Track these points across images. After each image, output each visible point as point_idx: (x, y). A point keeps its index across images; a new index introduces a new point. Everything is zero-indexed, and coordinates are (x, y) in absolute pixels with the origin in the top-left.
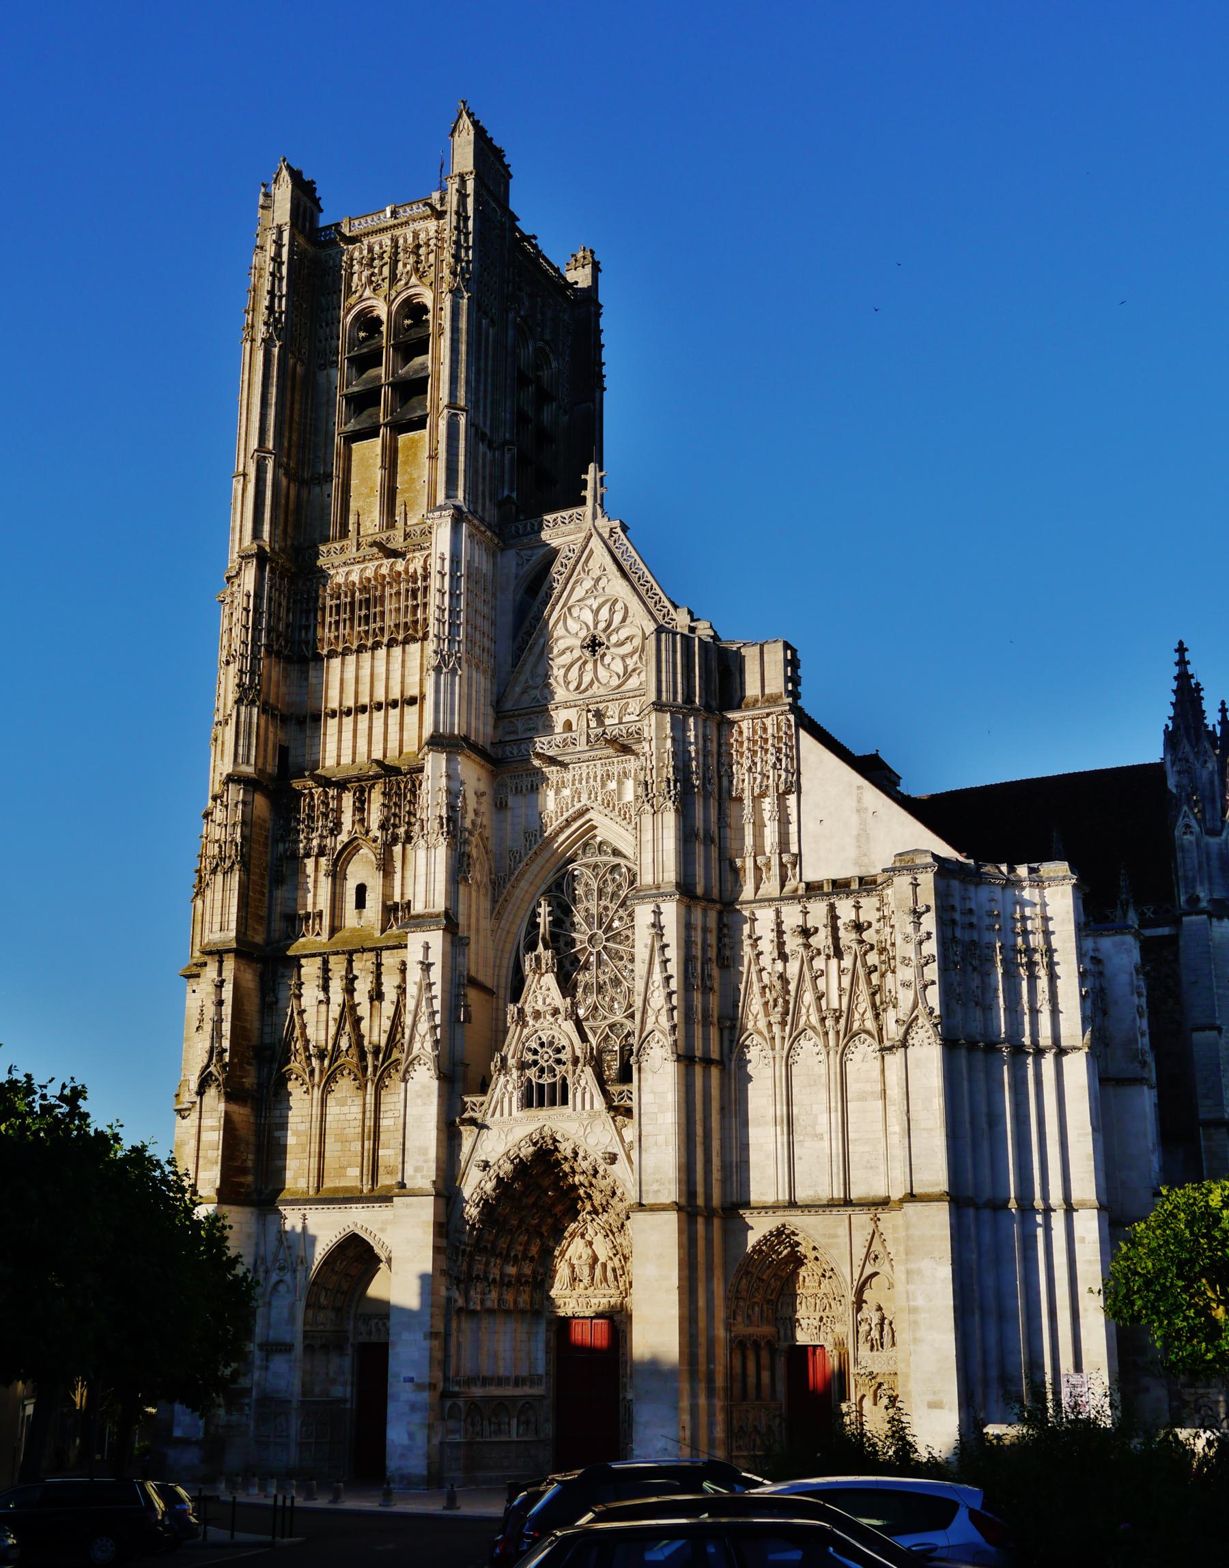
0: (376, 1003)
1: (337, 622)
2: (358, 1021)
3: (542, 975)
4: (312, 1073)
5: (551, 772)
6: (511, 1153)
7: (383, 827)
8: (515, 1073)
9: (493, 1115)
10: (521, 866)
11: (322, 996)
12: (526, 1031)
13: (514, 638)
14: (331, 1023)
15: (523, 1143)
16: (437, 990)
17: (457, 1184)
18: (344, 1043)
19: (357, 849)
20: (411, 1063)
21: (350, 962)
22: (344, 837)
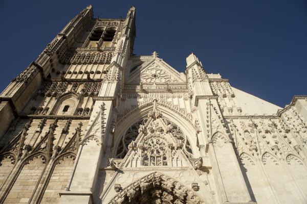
0: (64, 135)
1: (78, 59)
2: (53, 139)
3: (155, 119)
4: (20, 155)
5: (142, 94)
6: (135, 184)
7: (83, 90)
8: (140, 151)
9: (126, 166)
10: (129, 113)
11: (39, 129)
12: (145, 137)
13: (131, 72)
14: (40, 137)
15: (143, 180)
16: (107, 117)
17: (100, 197)
18: (43, 146)
19: (70, 97)
20: (88, 138)
21: (57, 121)
22: (67, 92)
